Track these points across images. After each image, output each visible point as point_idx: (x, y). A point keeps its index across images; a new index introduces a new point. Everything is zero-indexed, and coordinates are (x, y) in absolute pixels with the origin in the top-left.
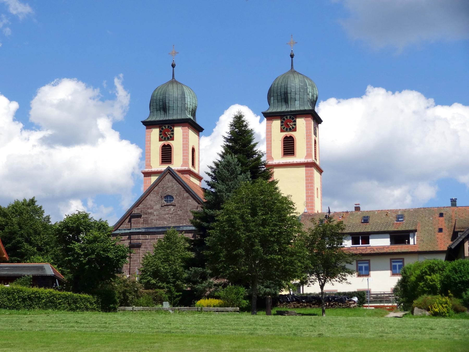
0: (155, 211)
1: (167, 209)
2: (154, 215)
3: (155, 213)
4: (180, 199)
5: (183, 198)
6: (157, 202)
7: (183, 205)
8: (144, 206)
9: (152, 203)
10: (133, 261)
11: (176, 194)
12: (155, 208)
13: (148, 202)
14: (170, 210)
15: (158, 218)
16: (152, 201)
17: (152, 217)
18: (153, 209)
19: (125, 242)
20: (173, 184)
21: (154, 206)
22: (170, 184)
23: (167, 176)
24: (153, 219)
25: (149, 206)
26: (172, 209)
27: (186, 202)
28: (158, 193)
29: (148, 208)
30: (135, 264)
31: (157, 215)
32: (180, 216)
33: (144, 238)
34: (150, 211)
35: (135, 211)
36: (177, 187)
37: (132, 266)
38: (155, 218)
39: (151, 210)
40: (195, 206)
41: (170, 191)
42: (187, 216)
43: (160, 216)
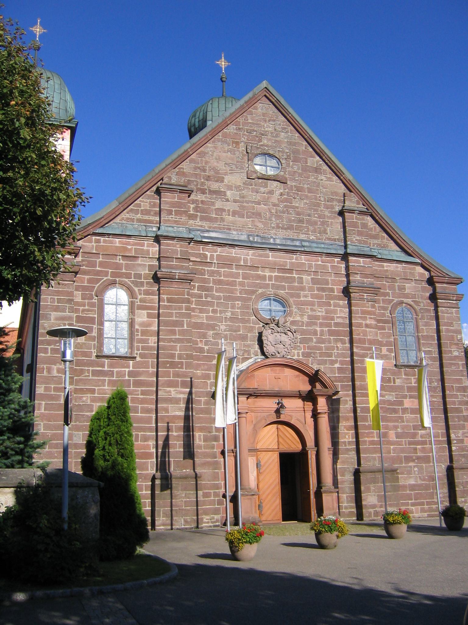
0: (230, 188)
1: (262, 189)
2: (227, 200)
3: (229, 193)
4: (298, 169)
5: (305, 169)
6: (234, 167)
7: (306, 186)
8: (196, 168)
9: (221, 166)
10: (167, 324)
11: (288, 156)
12: (227, 179)
13: (207, 163)
14: (271, 192)
15: (238, 209)
16: (218, 159)
17: (219, 204)
18: (222, 181)
19: (140, 265)
20: (278, 128)
21: (226, 174)
22: (269, 127)
23: (259, 105)
24: (224, 210)
25: (212, 173)
26: (278, 193)
27: (312, 179)
28: (237, 143)
29: (208, 178)
30: (173, 332)
31: (235, 201)
32: (298, 214)
33: (198, 260)
34: (215, 186)
35: (170, 178)
36: (287, 137)
37: (164, 340)
38: (230, 206)
39: (219, 184)
40: (336, 194)
41: (270, 143)
42: (316, 216)
43: (245, 204)
